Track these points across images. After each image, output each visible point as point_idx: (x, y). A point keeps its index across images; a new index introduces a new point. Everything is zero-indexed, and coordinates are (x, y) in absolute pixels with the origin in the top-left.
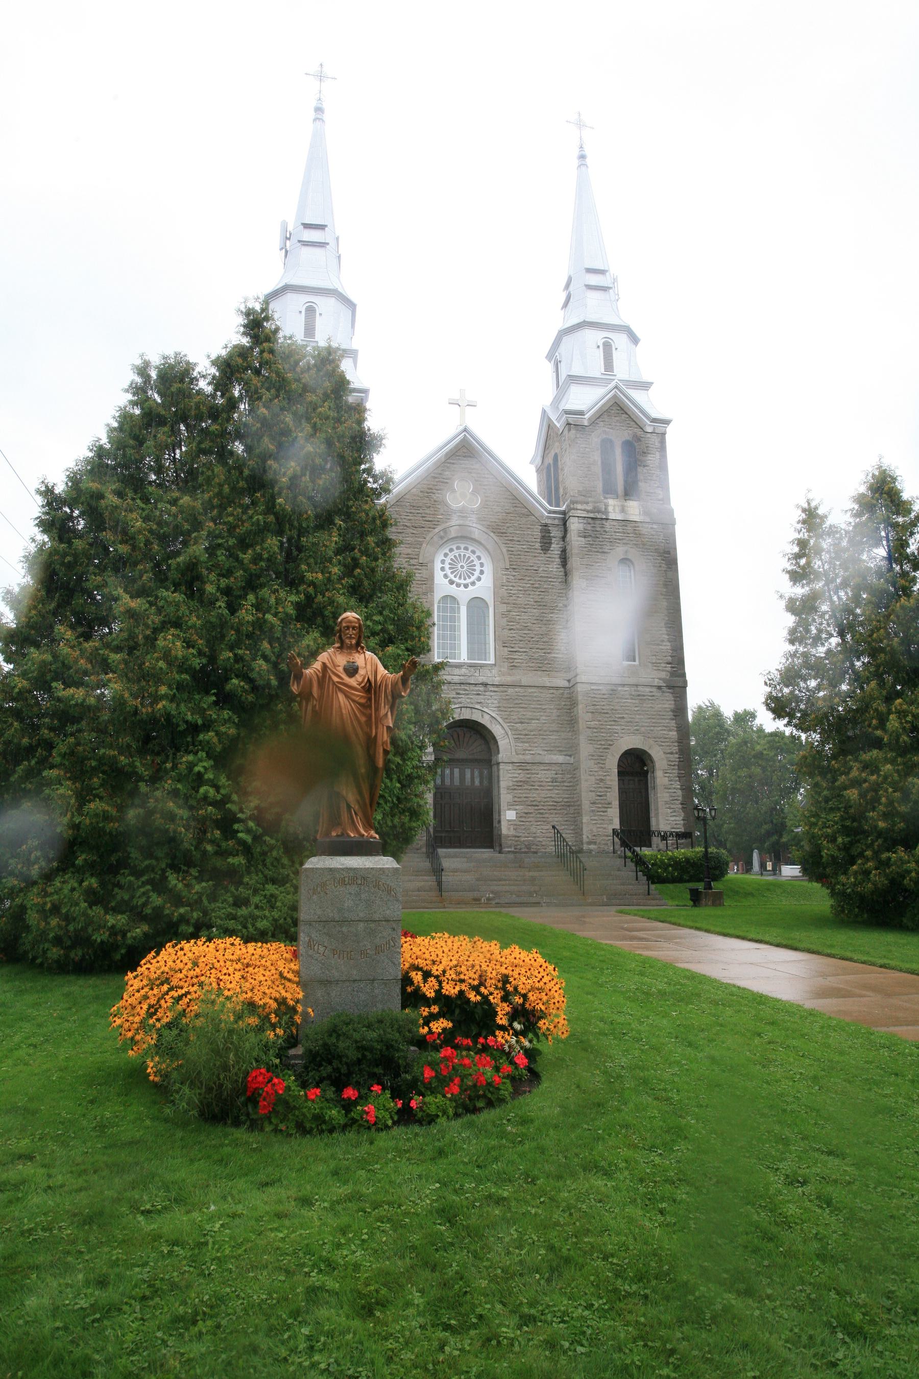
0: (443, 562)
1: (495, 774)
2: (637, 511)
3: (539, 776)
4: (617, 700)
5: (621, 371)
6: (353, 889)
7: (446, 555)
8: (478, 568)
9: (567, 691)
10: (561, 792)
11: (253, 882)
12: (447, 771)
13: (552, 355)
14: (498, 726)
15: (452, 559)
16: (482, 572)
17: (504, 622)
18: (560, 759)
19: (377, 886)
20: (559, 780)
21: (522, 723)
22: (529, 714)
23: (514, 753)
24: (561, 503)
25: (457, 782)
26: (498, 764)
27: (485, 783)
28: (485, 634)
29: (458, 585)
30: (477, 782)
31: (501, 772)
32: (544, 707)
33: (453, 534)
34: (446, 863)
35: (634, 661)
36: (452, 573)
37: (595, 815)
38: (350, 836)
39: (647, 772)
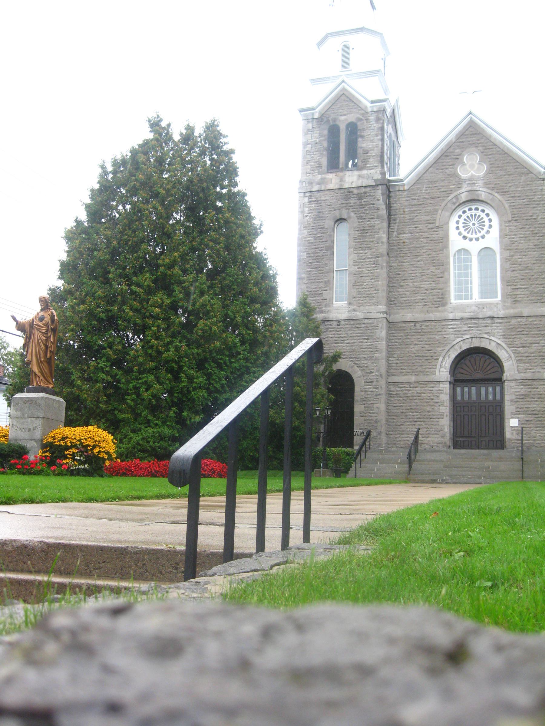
0: (458, 222)
3: (538, 390)
6: (28, 405)
7: (460, 216)
8: (487, 223)
12: (466, 389)
14: (503, 351)
16: (490, 226)
17: (508, 265)
21: (523, 347)
22: (530, 340)
25: (474, 397)
27: (498, 397)
28: (496, 277)
29: (471, 240)
30: (491, 397)
31: (506, 388)
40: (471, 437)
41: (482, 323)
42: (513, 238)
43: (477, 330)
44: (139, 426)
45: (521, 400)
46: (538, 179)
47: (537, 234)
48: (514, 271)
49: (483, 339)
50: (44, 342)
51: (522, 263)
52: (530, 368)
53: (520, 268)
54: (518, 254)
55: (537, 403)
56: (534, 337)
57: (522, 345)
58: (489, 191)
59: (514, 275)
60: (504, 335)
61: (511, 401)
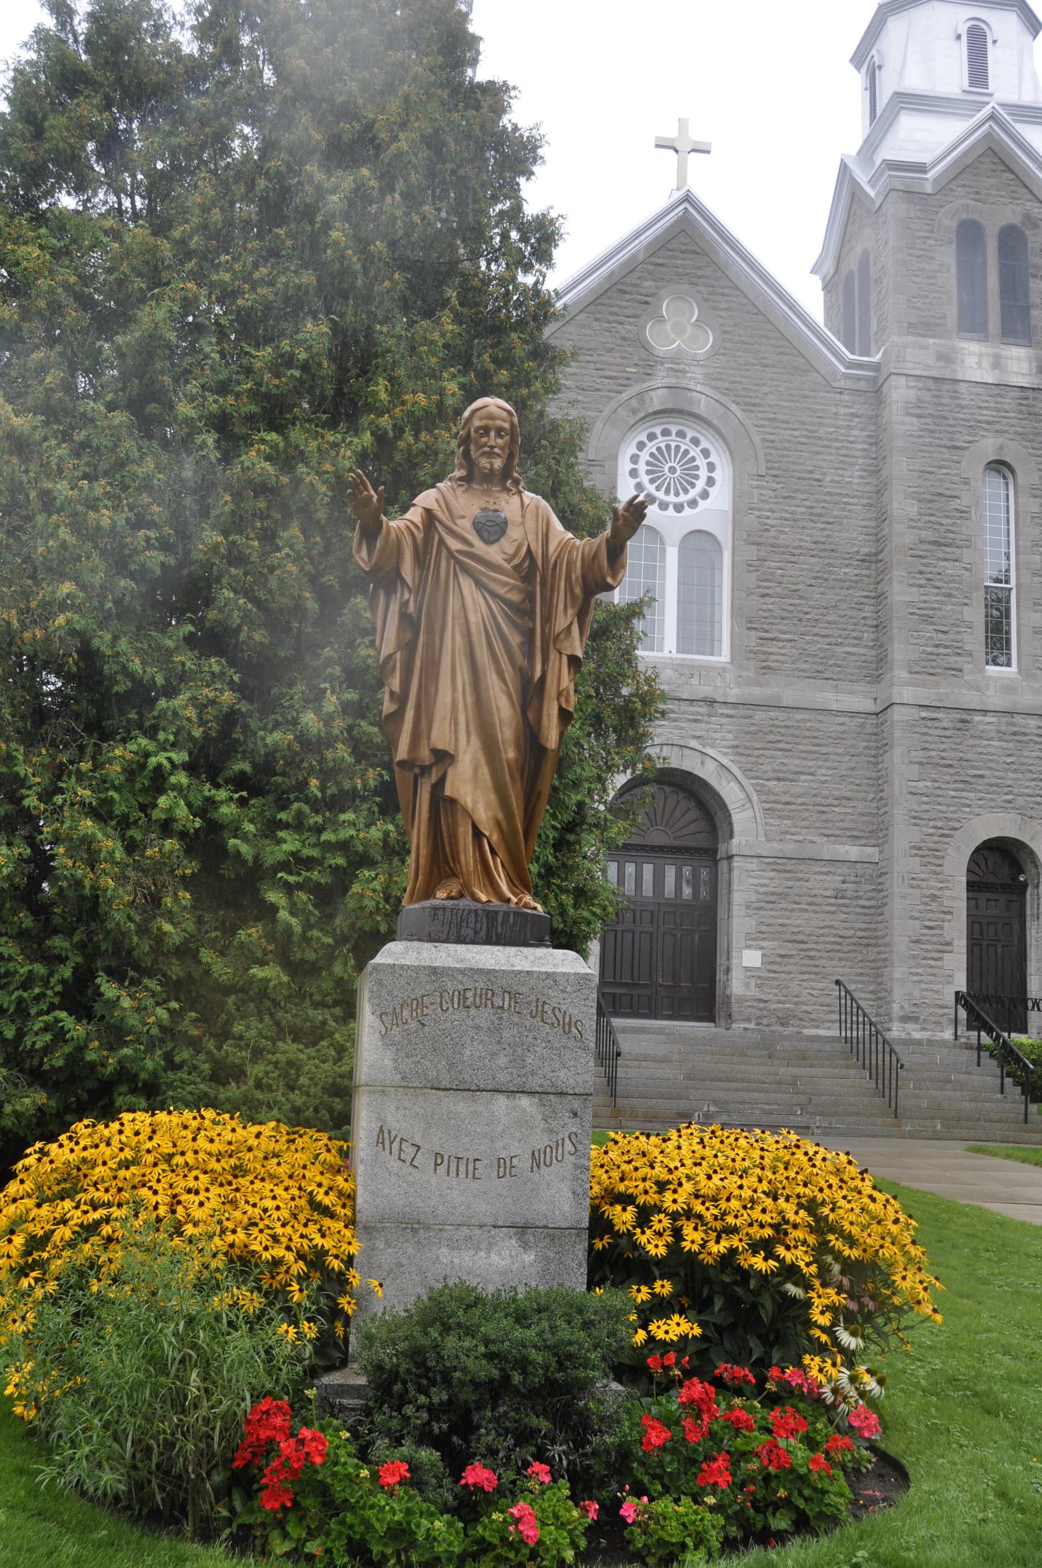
0: (635, 459)
1: (723, 878)
2: (1025, 367)
4: (971, 742)
5: (1006, 86)
6: (484, 1017)
7: (641, 446)
8: (703, 473)
9: (872, 720)
10: (852, 917)
11: (253, 1033)
13: (865, 57)
14: (732, 784)
15: (652, 455)
16: (711, 482)
18: (852, 851)
19: (539, 1012)
20: (849, 894)
21: (779, 779)
22: (794, 764)
23: (762, 839)
24: (873, 349)
25: (648, 890)
26: (730, 858)
27: (704, 893)
28: (714, 604)
31: (736, 873)
32: (824, 750)
33: (657, 406)
34: (626, 1044)
35: (1009, 665)
36: (652, 481)
37: (918, 966)
38: (478, 900)
39: (1024, 886)
40: (634, 985)
41: (685, 713)
42: (768, 518)
43: (675, 727)
44: (319, 1015)
45: (771, 906)
46: (829, 389)
47: (820, 515)
48: (763, 596)
49: (686, 752)
50: (520, 659)
51: (785, 579)
52: (793, 830)
53: (778, 590)
54: (777, 558)
55: (806, 915)
56: (805, 759)
57: (776, 775)
58: (718, 396)
59: (765, 607)
60: (737, 747)
61: (748, 907)
